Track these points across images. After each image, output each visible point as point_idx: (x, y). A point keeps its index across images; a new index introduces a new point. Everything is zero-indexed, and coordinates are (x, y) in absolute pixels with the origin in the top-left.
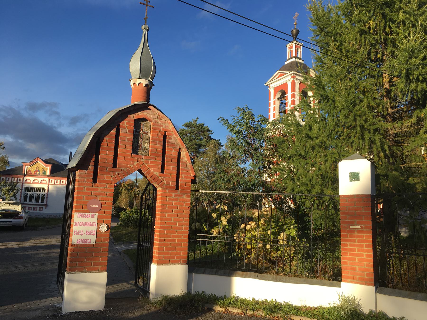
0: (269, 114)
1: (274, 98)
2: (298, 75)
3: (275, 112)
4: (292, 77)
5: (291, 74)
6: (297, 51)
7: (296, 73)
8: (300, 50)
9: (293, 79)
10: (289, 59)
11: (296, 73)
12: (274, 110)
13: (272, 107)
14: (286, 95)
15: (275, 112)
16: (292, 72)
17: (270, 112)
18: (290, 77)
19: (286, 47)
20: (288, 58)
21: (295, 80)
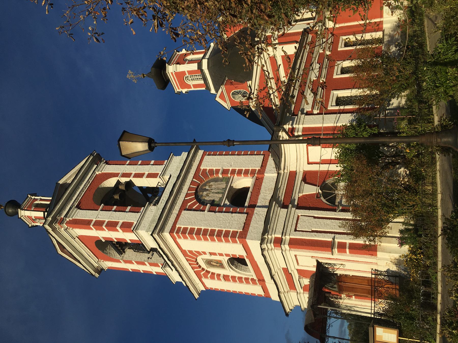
2: (60, 212)
5: (54, 229)
6: (38, 207)
7: (50, 219)
8: (39, 199)
11: (50, 219)
12: (143, 264)
13: (142, 268)
19: (33, 226)
21: (68, 220)
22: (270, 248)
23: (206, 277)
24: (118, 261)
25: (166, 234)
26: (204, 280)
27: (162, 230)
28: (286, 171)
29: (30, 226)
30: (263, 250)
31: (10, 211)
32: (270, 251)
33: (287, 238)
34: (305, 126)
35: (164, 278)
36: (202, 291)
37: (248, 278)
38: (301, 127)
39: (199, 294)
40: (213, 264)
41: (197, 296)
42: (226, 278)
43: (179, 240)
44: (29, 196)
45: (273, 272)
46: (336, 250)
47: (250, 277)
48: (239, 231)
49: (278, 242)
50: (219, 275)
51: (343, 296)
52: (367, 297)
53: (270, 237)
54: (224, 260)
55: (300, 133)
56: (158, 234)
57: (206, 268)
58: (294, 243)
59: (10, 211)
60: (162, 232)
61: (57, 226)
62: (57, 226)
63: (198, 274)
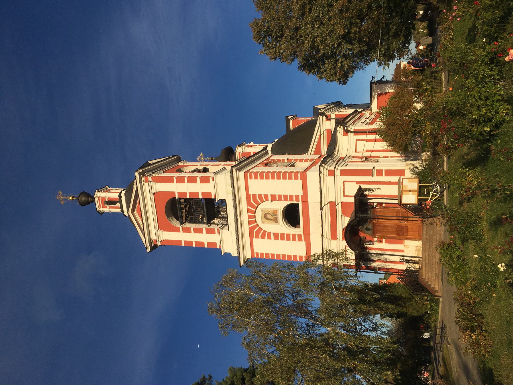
0: (206, 246)
1: (179, 231)
3: (204, 230)
4: (147, 181)
5: (140, 180)
7: (141, 171)
9: (150, 178)
10: (121, 207)
11: (141, 171)
14: (177, 198)
15: (204, 230)
16: (137, 174)
17: (203, 243)
18: (146, 185)
20: (119, 210)
22: (325, 174)
23: (257, 237)
24: (178, 230)
25: (241, 174)
26: (255, 240)
27: (239, 170)
28: (338, 155)
29: (98, 210)
30: (320, 172)
31: (83, 199)
32: (325, 176)
33: (340, 168)
34: (356, 128)
35: (213, 251)
36: (248, 259)
37: (295, 235)
38: (353, 128)
39: (245, 262)
40: (269, 217)
41: (242, 263)
42: (276, 236)
43: (249, 180)
44: (107, 187)
45: (323, 205)
46: (375, 172)
47: (297, 233)
48: (301, 171)
49: (331, 173)
50: (269, 233)
51: (376, 239)
52: (394, 238)
53: (326, 166)
54: (280, 206)
55: (352, 130)
56: (236, 170)
57: (261, 225)
58: (344, 173)
59: (83, 199)
60: (240, 171)
61: (143, 179)
62: (143, 179)
63: (251, 230)
